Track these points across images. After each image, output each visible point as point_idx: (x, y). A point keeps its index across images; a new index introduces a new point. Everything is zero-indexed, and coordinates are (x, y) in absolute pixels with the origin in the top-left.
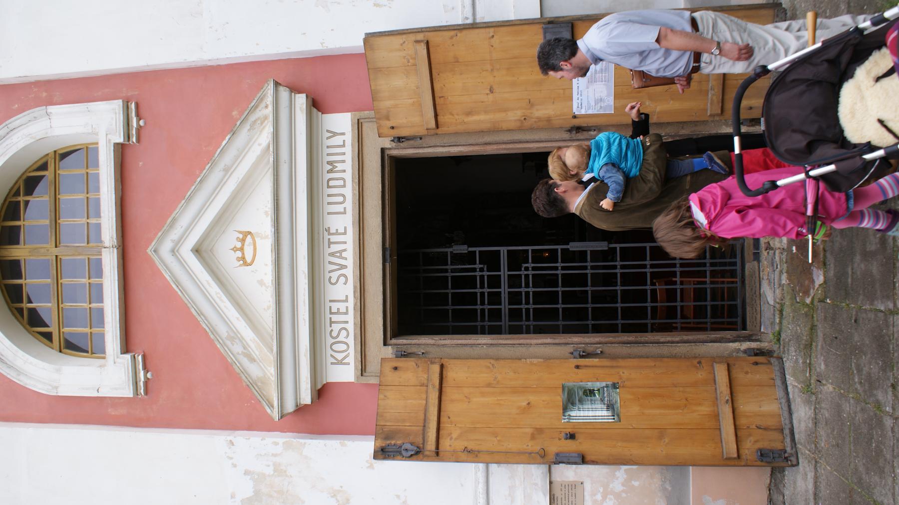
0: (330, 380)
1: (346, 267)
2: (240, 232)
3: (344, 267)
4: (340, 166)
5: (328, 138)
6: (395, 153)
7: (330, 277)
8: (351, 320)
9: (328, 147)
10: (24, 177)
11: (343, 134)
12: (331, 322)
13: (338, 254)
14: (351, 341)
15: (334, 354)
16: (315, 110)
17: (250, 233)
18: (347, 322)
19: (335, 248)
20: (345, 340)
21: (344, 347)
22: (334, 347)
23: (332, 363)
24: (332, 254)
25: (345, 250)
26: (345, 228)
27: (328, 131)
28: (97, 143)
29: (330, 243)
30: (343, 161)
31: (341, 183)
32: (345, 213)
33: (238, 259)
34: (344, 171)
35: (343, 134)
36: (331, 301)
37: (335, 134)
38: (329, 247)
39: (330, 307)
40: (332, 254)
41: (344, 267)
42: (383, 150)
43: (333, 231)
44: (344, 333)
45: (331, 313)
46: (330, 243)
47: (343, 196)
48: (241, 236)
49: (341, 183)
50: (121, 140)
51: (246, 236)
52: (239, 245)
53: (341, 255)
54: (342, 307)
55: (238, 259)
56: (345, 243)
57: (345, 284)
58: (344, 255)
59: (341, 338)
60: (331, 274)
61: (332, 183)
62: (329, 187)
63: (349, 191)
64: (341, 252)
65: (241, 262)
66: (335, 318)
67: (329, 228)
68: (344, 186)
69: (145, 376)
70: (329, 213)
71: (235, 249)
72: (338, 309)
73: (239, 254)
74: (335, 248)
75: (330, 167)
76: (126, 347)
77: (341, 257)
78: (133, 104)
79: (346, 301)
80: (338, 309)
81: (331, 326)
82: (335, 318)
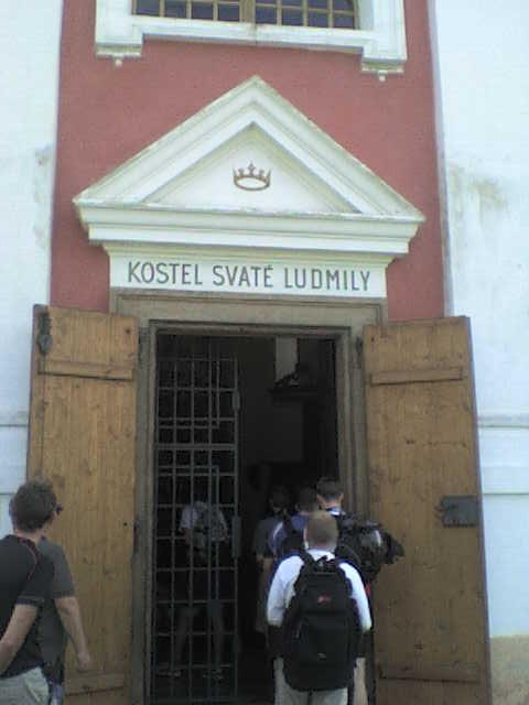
2: (269, 175)
4: (333, 283)
6: (345, 340)
11: (365, 288)
14: (154, 285)
15: (139, 268)
16: (390, 260)
17: (268, 185)
18: (174, 282)
20: (155, 278)
21: (148, 277)
22: (148, 267)
23: (130, 264)
24: (244, 270)
25: (249, 284)
26: (271, 286)
27: (368, 273)
28: (359, 28)
29: (256, 269)
30: (338, 288)
31: (317, 284)
32: (287, 286)
35: (365, 288)
37: (365, 281)
38: (252, 268)
39: (189, 265)
40: (244, 270)
42: (349, 328)
43: (268, 273)
44: (163, 278)
46: (256, 269)
47: (303, 286)
48: (265, 175)
49: (317, 284)
50: (367, 54)
51: (264, 181)
52: (256, 173)
55: (241, 171)
57: (215, 283)
58: (244, 283)
59: (157, 275)
60: (224, 269)
61: (317, 274)
62: (313, 271)
64: (247, 280)
65: (238, 174)
66: (179, 270)
68: (314, 287)
69: (119, 58)
71: (251, 168)
73: (247, 172)
75: (332, 273)
76: (150, 42)
77: (242, 280)
79: (197, 283)
82: (179, 270)
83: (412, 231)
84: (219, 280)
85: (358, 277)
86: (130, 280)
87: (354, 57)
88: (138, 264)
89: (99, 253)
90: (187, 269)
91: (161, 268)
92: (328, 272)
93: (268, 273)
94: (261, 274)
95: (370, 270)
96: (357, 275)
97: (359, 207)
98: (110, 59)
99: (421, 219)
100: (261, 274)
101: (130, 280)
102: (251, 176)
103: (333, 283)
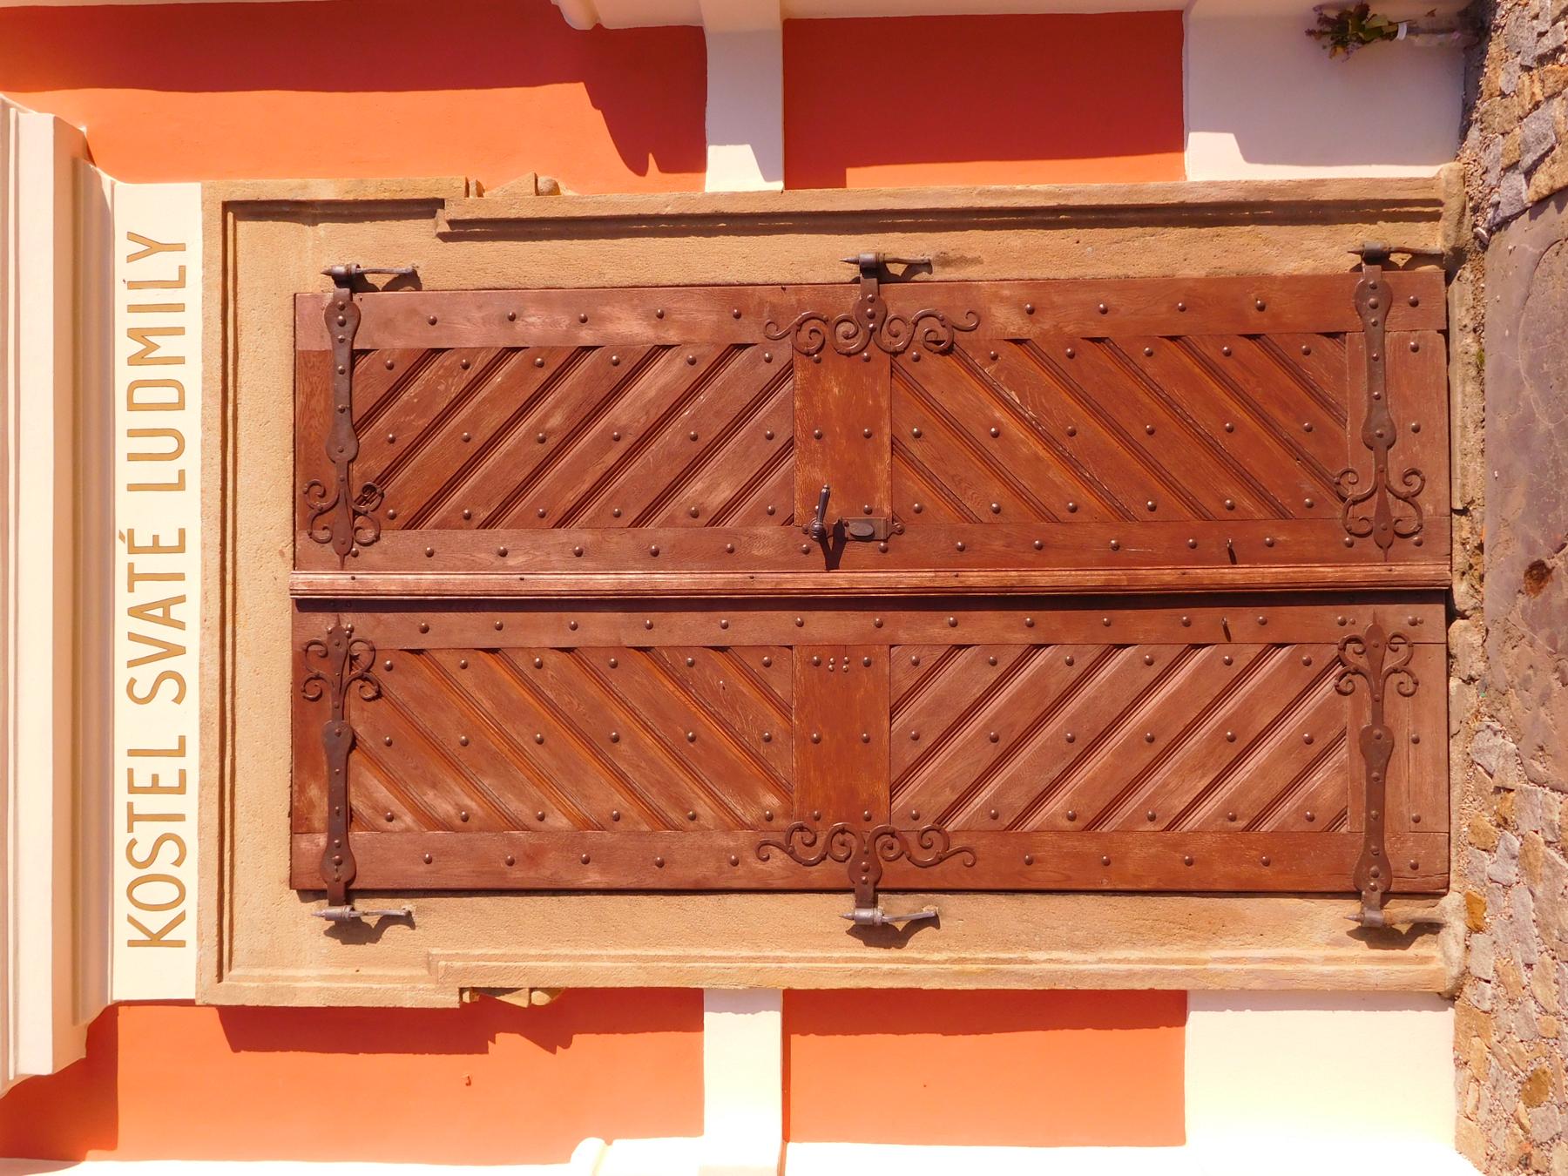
1: (179, 651)
3: (175, 650)
4: (167, 347)
5: (131, 258)
7: (132, 682)
11: (181, 247)
13: (159, 612)
14: (189, 874)
15: (140, 915)
18: (180, 818)
19: (148, 592)
21: (168, 892)
22: (138, 893)
23: (132, 943)
24: (137, 612)
25: (181, 599)
26: (182, 533)
27: (132, 237)
30: (179, 331)
31: (170, 395)
32: (180, 486)
34: (180, 361)
35: (181, 247)
37: (153, 247)
38: (131, 589)
39: (130, 772)
40: (137, 612)
41: (175, 650)
43: (142, 540)
44: (169, 850)
45: (132, 789)
49: (170, 395)
53: (167, 612)
54: (168, 771)
56: (180, 577)
57: (178, 699)
58: (176, 612)
60: (136, 672)
61: (141, 396)
62: (132, 406)
64: (166, 604)
67: (131, 532)
68: (180, 405)
72: (155, 778)
75: (138, 347)
77: (167, 620)
79: (181, 751)
80: (155, 778)
81: (130, 829)
84: (170, 687)
86: (180, 944)
88: (131, 920)
90: (142, 780)
91: (141, 853)
92: (134, 361)
93: (142, 540)
94: (144, 563)
101: (180, 944)
103: (167, 346)
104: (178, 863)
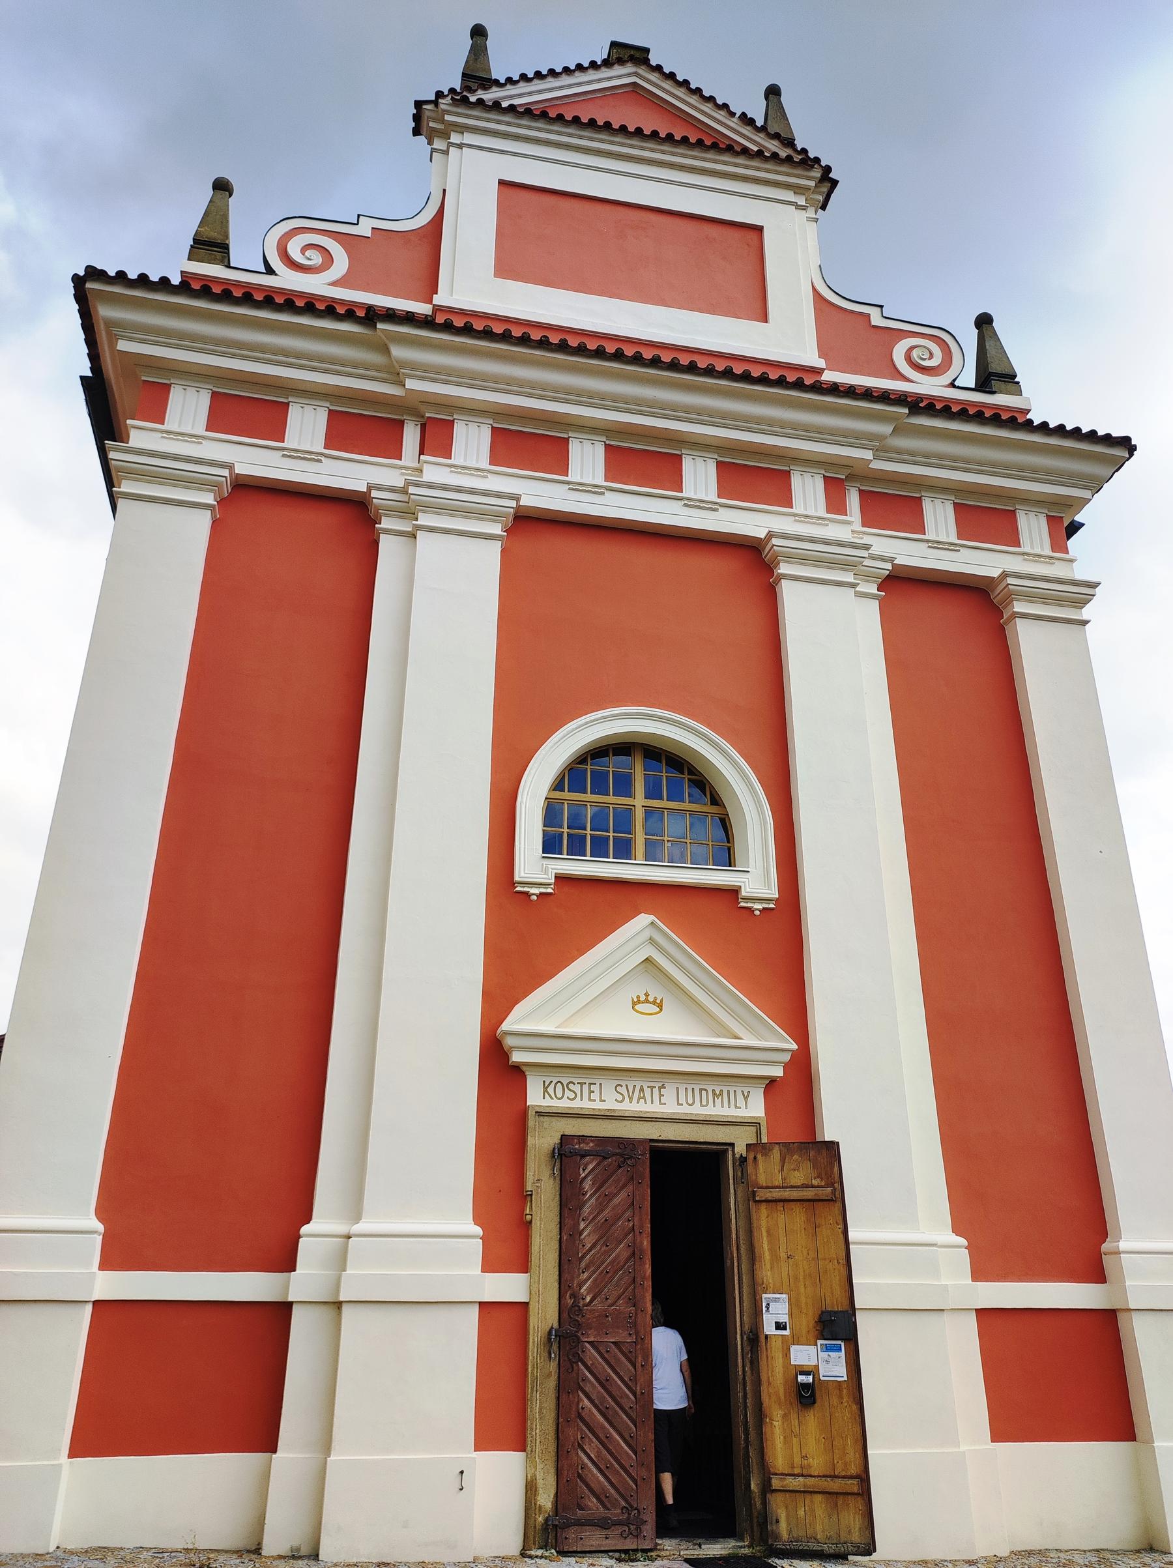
0: (528, 1077)
3: (631, 1098)
4: (718, 1102)
8: (582, 1104)
9: (735, 1091)
10: (705, 781)
12: (582, 1084)
13: (642, 1095)
15: (553, 1084)
17: (661, 1010)
19: (647, 1091)
21: (559, 1095)
23: (544, 1082)
24: (642, 1090)
27: (749, 1092)
29: (652, 1088)
31: (704, 1103)
32: (679, 1104)
33: (638, 997)
36: (601, 1084)
37: (746, 1099)
38: (648, 1087)
39: (595, 1084)
40: (642, 1090)
41: (631, 1098)
42: (732, 1145)
44: (572, 1095)
45: (590, 1084)
46: (652, 1088)
48: (658, 1001)
50: (744, 893)
52: (651, 999)
53: (642, 1098)
54: (594, 1096)
55: (638, 997)
59: (567, 1092)
60: (624, 1087)
61: (704, 1093)
62: (701, 1090)
63: (697, 1110)
64: (644, 1097)
66: (585, 1087)
67: (665, 1088)
68: (702, 1105)
69: (533, 894)
70: (678, 1088)
71: (647, 995)
72: (593, 1092)
73: (643, 998)
74: (647, 1091)
76: (560, 879)
78: (774, 906)
79: (601, 1100)
80: (593, 1092)
81: (578, 1083)
82: (585, 1087)
83: (787, 1057)
85: (739, 1095)
87: (733, 893)
89: (518, 1072)
94: (656, 1091)
95: (749, 1089)
96: (739, 1095)
97: (741, 1035)
98: (527, 894)
99: (795, 1046)
100: (656, 1091)
102: (647, 1001)
104: (568, 1098)
